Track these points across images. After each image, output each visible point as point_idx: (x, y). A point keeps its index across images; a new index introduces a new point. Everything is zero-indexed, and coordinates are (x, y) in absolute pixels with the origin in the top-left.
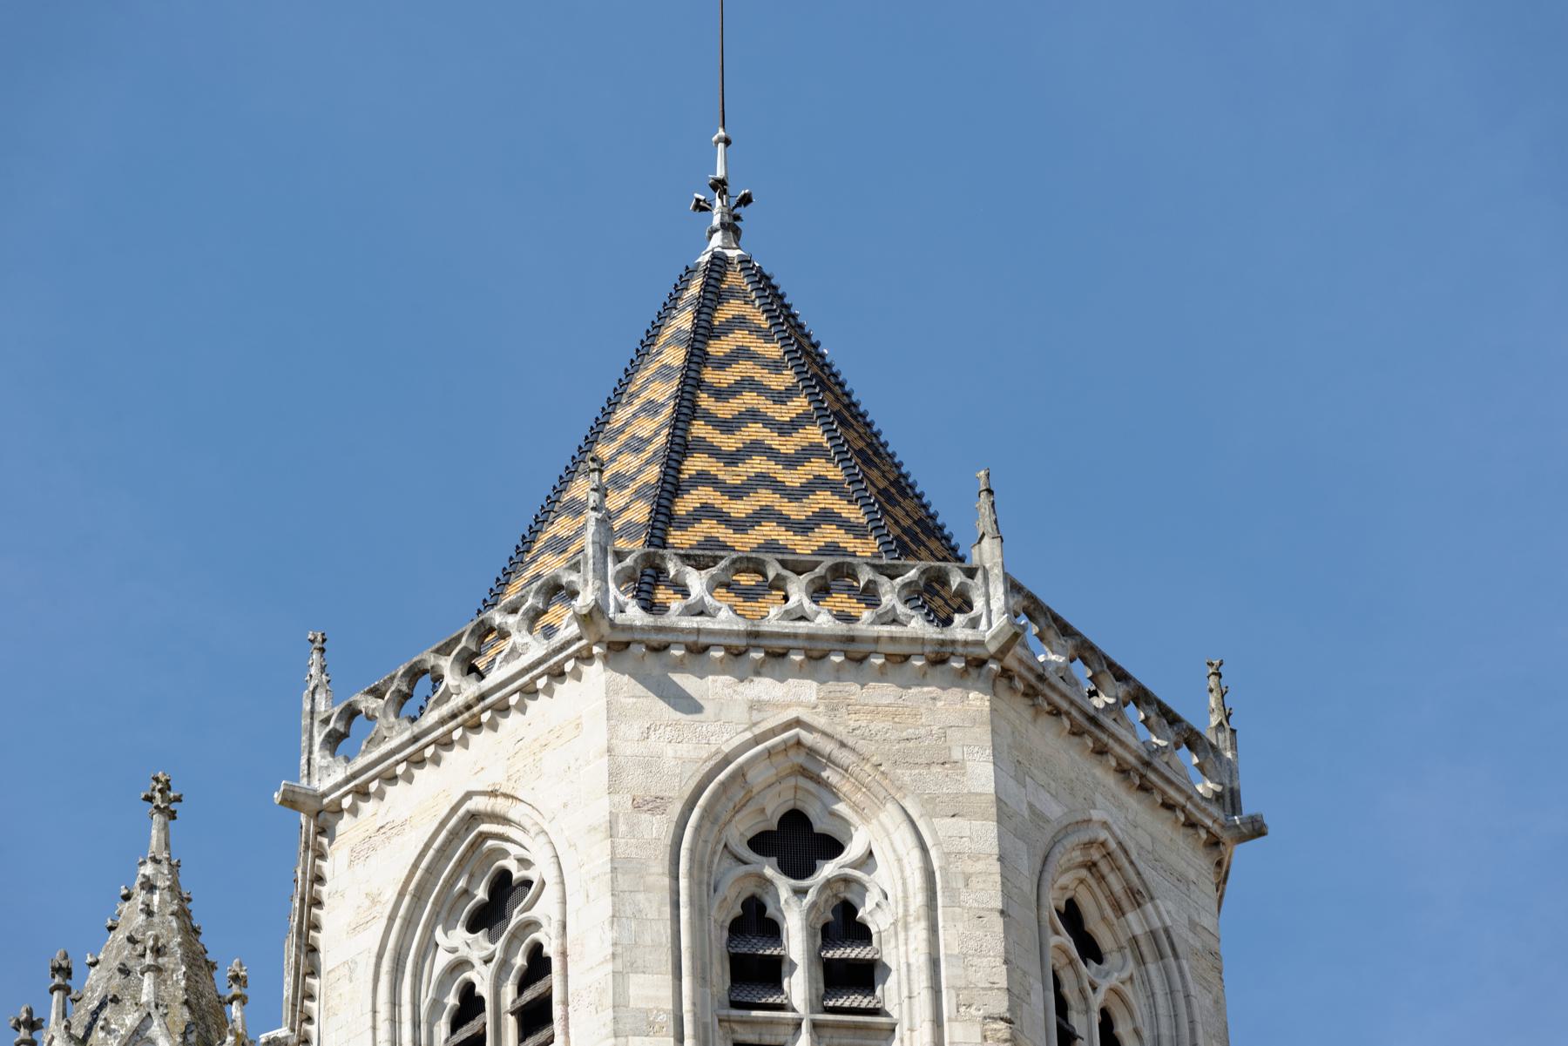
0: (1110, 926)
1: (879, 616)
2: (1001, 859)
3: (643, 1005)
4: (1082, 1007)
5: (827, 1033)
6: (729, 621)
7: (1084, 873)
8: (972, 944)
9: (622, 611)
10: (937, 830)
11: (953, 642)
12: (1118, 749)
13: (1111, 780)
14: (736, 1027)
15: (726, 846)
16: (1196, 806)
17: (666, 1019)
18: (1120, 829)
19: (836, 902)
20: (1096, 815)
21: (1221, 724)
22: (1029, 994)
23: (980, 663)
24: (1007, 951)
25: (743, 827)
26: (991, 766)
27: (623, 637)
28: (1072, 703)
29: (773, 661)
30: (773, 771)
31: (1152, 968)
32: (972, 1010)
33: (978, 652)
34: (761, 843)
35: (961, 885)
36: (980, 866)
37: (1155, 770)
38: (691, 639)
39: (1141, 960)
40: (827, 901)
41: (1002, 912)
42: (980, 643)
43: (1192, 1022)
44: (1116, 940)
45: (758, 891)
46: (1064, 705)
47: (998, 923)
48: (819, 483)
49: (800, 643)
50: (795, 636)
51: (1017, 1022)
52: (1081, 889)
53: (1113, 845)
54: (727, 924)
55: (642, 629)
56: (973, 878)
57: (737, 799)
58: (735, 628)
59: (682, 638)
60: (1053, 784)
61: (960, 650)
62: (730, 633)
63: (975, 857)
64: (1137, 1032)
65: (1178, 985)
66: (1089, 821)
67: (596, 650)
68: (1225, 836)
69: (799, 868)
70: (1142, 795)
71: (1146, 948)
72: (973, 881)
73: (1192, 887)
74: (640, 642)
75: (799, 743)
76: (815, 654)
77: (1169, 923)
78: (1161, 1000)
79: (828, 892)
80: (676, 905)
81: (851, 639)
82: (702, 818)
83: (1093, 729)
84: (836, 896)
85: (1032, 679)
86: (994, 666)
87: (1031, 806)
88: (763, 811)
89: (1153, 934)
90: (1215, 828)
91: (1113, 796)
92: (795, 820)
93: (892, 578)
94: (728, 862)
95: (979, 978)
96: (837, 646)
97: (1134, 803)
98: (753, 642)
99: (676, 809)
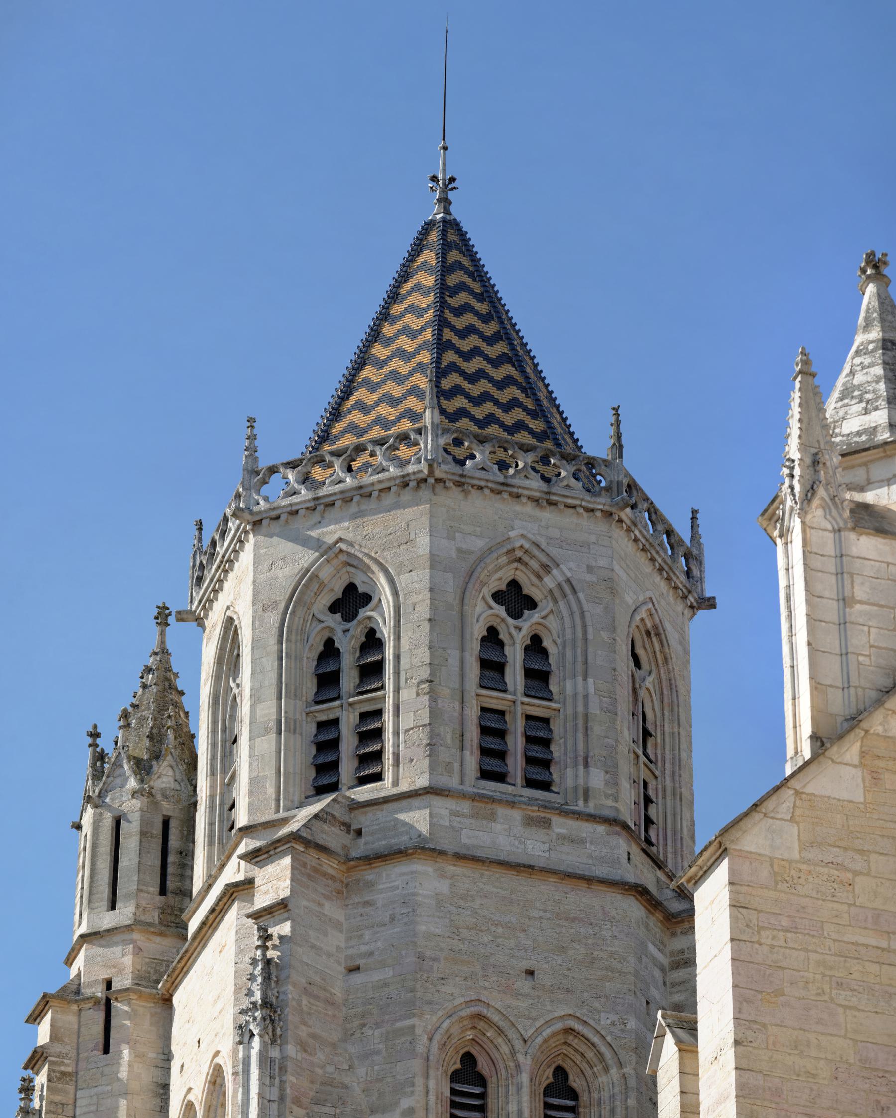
0: (537, 587)
1: (374, 470)
2: (431, 590)
3: (262, 720)
4: (511, 642)
5: (357, 706)
6: (304, 495)
7: (516, 565)
8: (415, 642)
9: (258, 504)
10: (403, 580)
11: (408, 475)
12: (526, 492)
13: (529, 508)
14: (316, 715)
15: (313, 615)
16: (589, 501)
17: (273, 725)
18: (534, 534)
19: (367, 631)
20: (512, 534)
21: (614, 444)
22: (447, 660)
23: (425, 480)
24: (431, 641)
25: (326, 600)
26: (428, 538)
27: (258, 518)
28: (487, 481)
29: (330, 508)
30: (333, 568)
31: (562, 604)
32: (413, 680)
33: (421, 476)
34: (334, 608)
35: (411, 610)
36: (420, 597)
37: (554, 494)
38: (289, 509)
39: (555, 601)
40: (361, 631)
41: (430, 620)
42: (421, 471)
43: (585, 626)
44: (543, 593)
45: (330, 635)
46: (483, 483)
47: (426, 626)
48: (420, 367)
49: (338, 496)
50: (335, 494)
51: (436, 681)
52: (518, 572)
53: (527, 546)
54: (316, 658)
55: (265, 511)
56: (417, 605)
57: (315, 590)
58: (307, 498)
59: (285, 510)
60: (478, 529)
61: (412, 477)
62: (305, 501)
63: (418, 592)
64: (554, 641)
65: (575, 608)
66: (509, 539)
67: (248, 528)
68: (613, 510)
69: (350, 617)
70: (552, 507)
71: (557, 593)
72: (417, 608)
73: (592, 546)
74: (267, 518)
75: (341, 551)
76: (349, 499)
77: (569, 574)
78: (567, 620)
79: (362, 626)
80: (281, 659)
81: (361, 487)
82: (294, 607)
83: (505, 488)
84: (366, 627)
85: (458, 478)
86: (431, 480)
87: (460, 551)
88: (332, 590)
89: (559, 585)
90: (607, 508)
91: (530, 517)
92: (351, 588)
93: (383, 445)
94: (315, 623)
95: (416, 661)
96: (355, 493)
97: (547, 515)
98: (317, 502)
99: (282, 606)
